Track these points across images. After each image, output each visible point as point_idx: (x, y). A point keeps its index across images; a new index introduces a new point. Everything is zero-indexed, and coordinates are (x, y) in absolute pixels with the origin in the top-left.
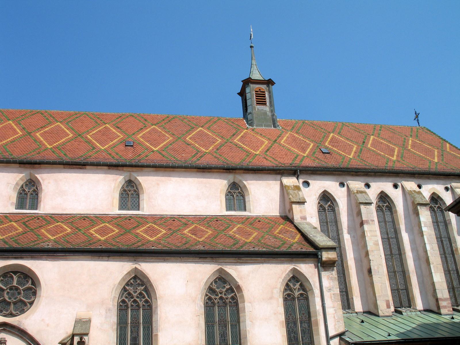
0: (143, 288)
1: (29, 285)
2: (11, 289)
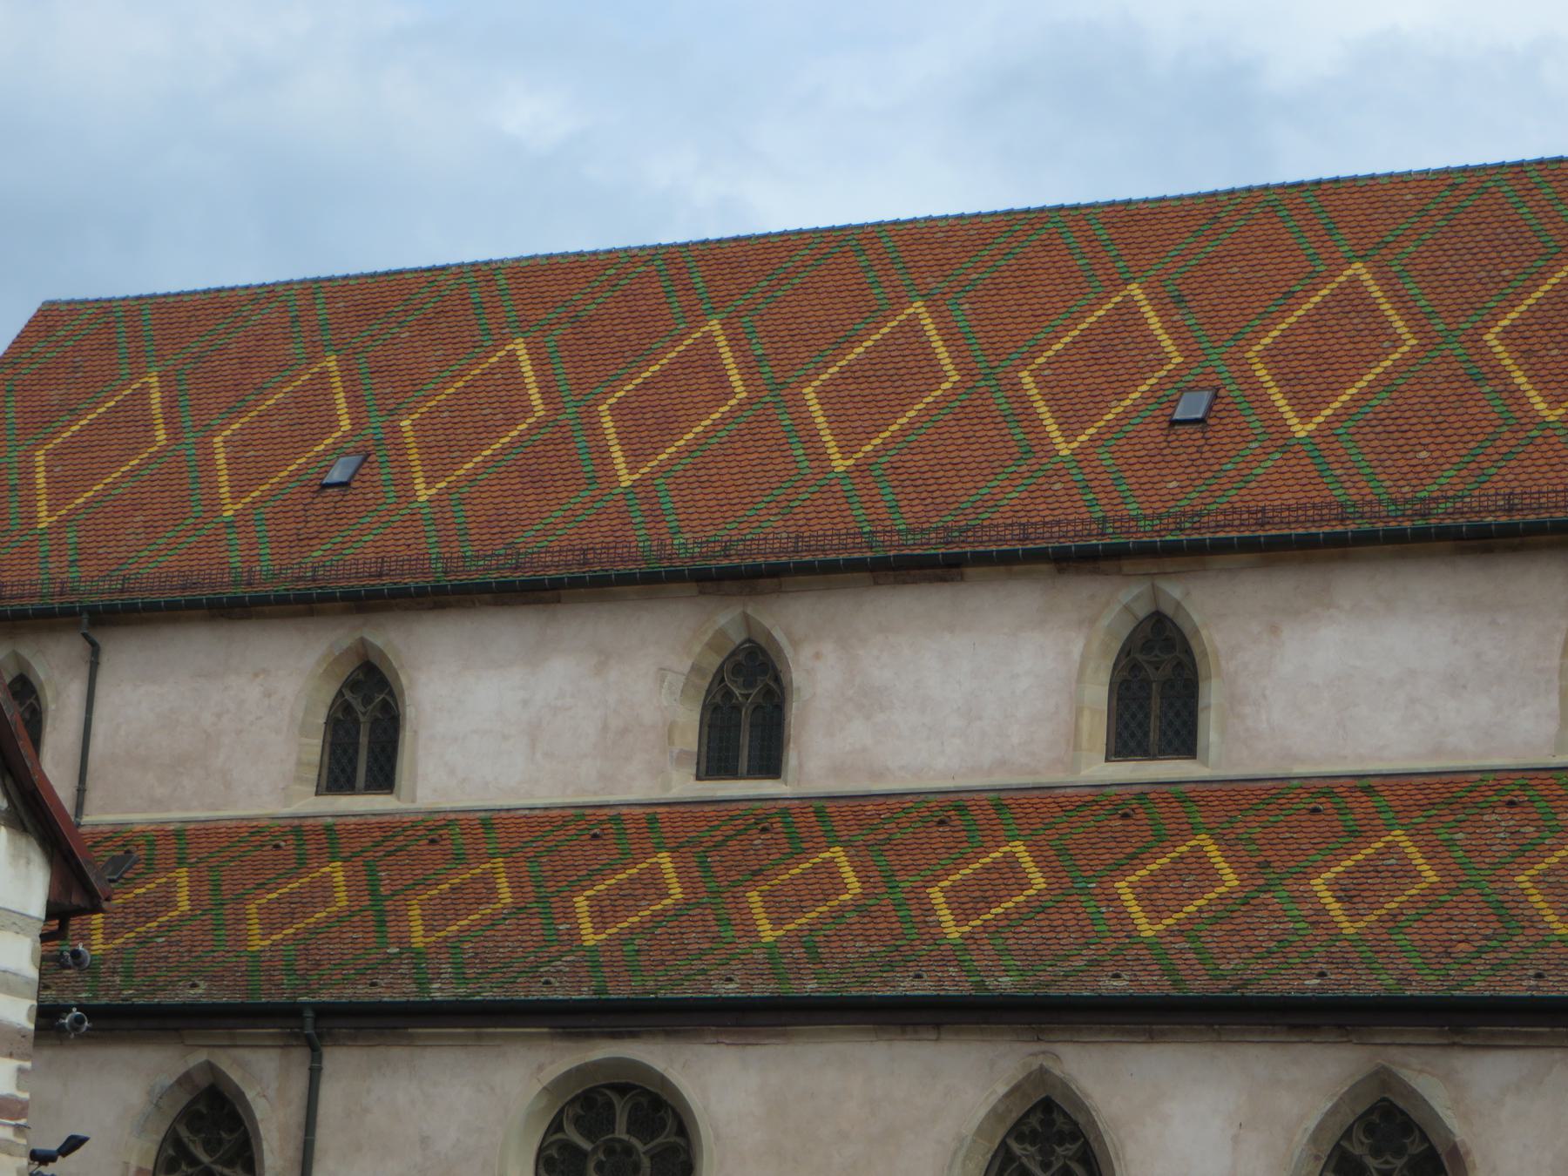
0: (1074, 1147)
1: (666, 1138)
2: (610, 1151)
